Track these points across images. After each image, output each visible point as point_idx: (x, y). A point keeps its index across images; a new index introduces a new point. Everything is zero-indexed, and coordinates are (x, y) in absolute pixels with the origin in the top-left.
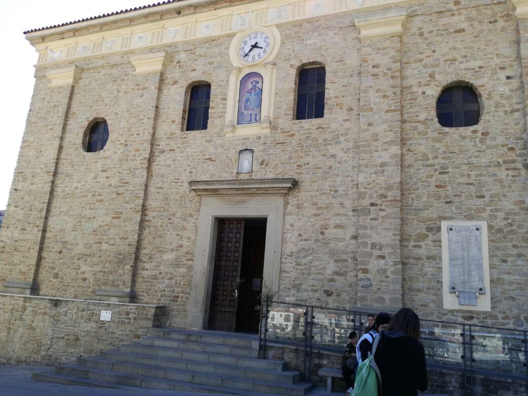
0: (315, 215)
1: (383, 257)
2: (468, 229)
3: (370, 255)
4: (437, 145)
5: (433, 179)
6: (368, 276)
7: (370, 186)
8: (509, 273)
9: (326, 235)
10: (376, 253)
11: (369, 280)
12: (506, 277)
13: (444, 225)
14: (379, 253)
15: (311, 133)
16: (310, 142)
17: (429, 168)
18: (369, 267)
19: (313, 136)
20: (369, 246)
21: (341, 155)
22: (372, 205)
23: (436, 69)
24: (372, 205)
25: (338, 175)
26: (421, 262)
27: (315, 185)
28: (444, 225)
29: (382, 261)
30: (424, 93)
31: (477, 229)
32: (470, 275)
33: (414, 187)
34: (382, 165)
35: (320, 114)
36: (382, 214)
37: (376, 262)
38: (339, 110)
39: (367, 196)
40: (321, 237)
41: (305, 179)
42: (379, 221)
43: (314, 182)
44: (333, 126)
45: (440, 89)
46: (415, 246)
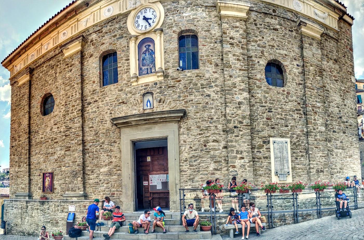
0: (200, 134)
1: (242, 158)
2: (282, 142)
3: (236, 157)
4: (267, 95)
5: (265, 115)
6: (236, 169)
7: (233, 116)
8: (298, 164)
9: (208, 147)
10: (239, 156)
11: (236, 171)
12: (297, 166)
13: (271, 140)
14: (241, 156)
15: (192, 80)
16: (192, 86)
17: (263, 108)
18: (235, 164)
19: (194, 81)
20: (235, 152)
21: (213, 94)
22: (235, 127)
23: (264, 49)
24: (235, 127)
25: (212, 108)
26: (260, 160)
27: (198, 115)
28: (271, 140)
29: (243, 161)
30: (258, 62)
31: (286, 143)
32: (284, 165)
33: (256, 118)
34: (240, 103)
35: (196, 66)
36: (241, 133)
37: (239, 161)
38: (209, 65)
39: (232, 122)
40: (204, 148)
41: (191, 110)
42: (240, 137)
43: (197, 113)
44: (207, 76)
45: (267, 62)
46: (258, 152)
